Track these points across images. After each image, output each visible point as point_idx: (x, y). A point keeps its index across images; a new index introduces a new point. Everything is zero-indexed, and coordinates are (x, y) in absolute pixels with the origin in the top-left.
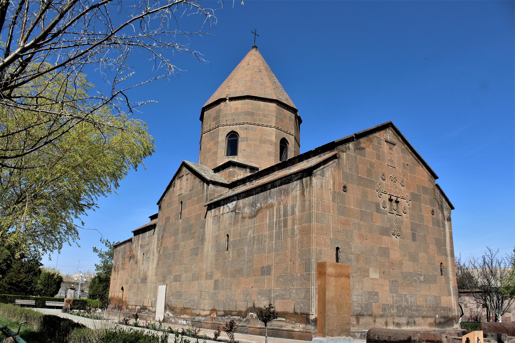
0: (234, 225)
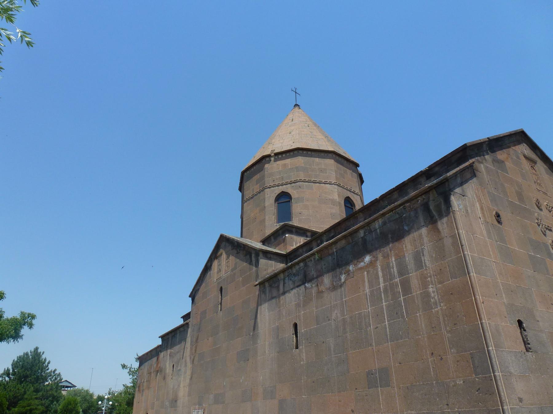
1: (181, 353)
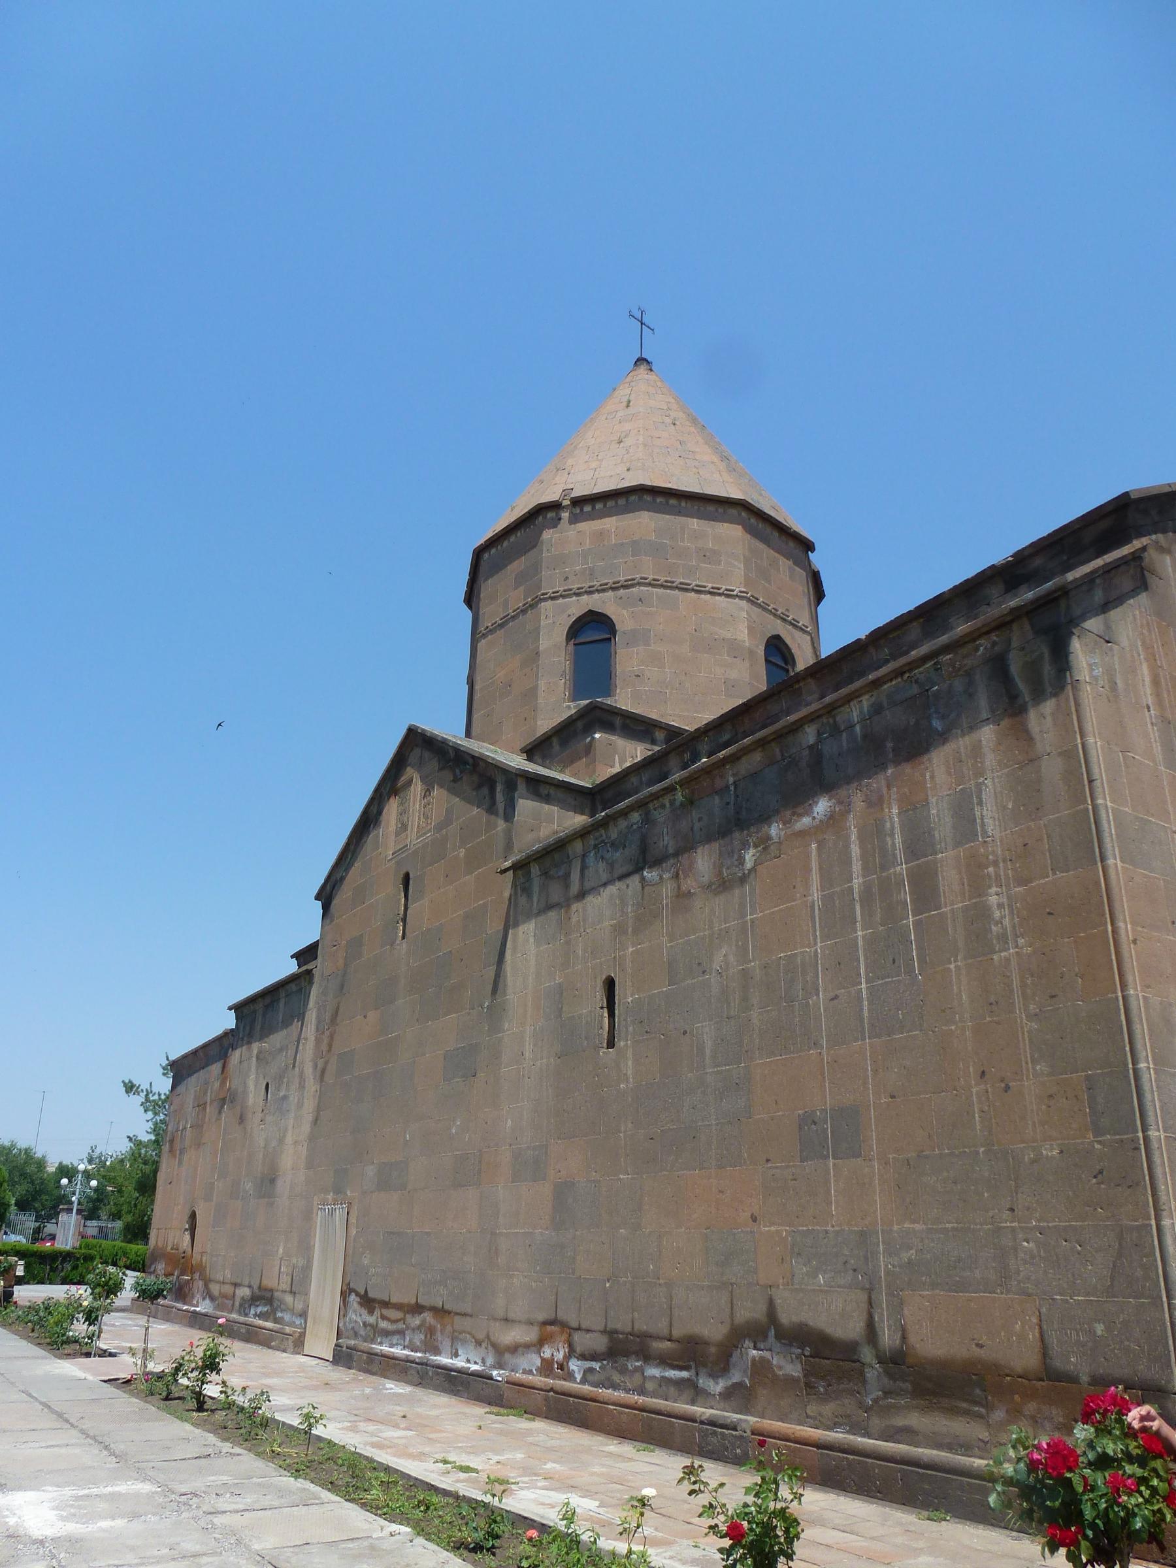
0: (636, 931)
1: (289, 1051)
